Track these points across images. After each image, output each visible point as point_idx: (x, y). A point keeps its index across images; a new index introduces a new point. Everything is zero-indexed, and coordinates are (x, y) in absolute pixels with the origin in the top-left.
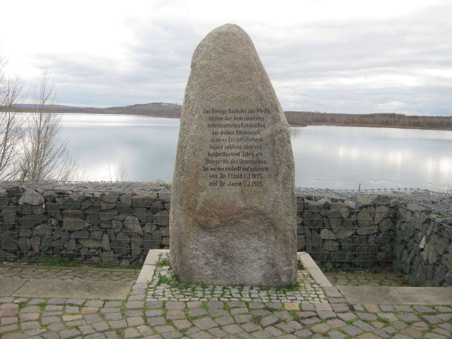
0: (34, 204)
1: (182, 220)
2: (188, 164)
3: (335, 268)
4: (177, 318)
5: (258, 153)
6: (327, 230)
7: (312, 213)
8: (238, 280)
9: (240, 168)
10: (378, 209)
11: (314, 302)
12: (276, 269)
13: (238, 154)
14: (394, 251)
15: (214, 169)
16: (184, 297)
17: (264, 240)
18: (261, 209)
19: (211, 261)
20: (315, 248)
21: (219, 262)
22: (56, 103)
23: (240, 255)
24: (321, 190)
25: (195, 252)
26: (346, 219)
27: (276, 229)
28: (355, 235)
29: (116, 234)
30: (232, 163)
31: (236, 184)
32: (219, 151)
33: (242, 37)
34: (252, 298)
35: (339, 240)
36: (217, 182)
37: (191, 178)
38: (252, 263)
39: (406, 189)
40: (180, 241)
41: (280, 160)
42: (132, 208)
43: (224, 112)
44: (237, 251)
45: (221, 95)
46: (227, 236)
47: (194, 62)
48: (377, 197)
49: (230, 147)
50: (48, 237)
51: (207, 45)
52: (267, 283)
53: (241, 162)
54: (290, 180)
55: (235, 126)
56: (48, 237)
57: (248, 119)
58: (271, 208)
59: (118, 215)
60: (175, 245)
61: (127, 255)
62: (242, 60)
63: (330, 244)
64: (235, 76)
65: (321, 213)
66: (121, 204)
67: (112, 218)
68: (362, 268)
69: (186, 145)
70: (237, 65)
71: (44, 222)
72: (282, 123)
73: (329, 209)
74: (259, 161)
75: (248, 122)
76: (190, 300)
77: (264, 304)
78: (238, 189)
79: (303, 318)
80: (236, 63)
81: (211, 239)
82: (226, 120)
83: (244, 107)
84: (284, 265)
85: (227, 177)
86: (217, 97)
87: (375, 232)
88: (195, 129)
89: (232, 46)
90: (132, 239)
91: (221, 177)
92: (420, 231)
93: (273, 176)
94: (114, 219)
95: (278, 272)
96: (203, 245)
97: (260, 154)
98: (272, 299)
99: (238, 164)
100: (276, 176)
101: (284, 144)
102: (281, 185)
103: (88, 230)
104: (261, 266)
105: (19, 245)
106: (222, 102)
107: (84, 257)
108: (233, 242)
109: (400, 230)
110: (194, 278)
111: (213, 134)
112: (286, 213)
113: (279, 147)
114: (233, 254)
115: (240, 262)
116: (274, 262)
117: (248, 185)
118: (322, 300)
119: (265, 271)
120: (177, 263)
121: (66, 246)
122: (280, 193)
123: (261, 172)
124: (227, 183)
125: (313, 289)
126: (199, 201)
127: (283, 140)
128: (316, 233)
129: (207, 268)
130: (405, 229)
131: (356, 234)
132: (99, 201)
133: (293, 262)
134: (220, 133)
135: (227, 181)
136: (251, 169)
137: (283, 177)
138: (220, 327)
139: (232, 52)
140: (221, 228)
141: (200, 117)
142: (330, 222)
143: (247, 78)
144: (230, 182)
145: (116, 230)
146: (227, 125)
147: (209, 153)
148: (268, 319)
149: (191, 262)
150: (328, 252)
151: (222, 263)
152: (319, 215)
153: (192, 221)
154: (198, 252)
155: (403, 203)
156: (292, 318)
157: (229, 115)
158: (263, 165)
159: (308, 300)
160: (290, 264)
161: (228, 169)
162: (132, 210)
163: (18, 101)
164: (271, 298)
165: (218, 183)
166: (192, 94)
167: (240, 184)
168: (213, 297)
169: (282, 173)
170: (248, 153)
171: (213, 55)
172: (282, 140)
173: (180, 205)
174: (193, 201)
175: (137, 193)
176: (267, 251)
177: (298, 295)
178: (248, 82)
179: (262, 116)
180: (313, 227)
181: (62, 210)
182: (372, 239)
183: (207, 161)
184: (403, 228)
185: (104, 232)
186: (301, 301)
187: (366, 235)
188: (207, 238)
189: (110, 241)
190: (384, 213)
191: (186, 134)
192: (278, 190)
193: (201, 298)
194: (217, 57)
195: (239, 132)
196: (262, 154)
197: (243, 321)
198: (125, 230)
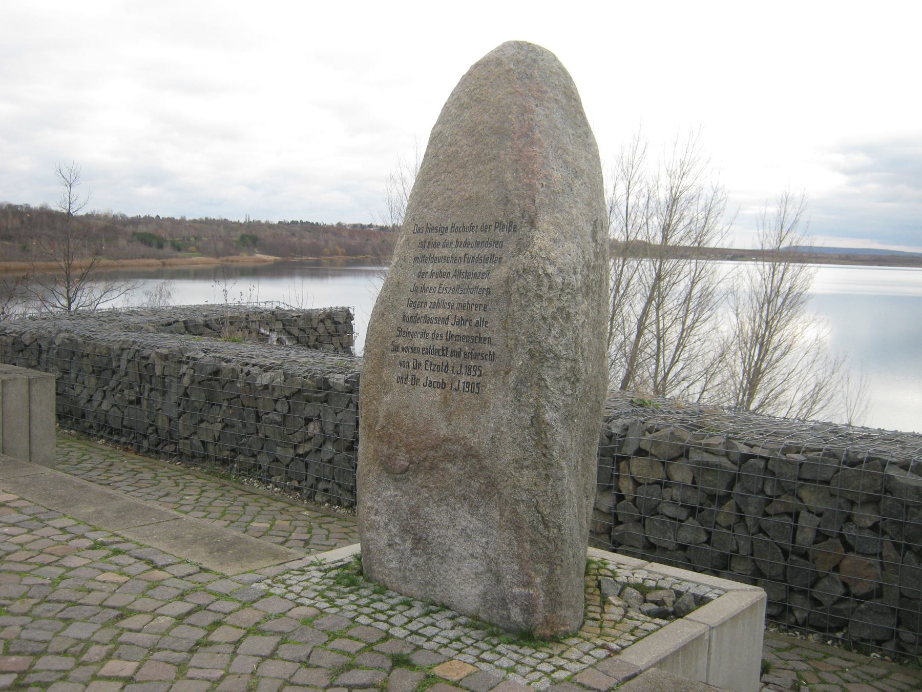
5: (479, 319)
8: (438, 595)
9: (447, 351)
13: (445, 320)
22: (805, 243)
25: (373, 517)
41: (516, 338)
43: (443, 230)
44: (433, 530)
46: (419, 494)
54: (532, 385)
57: (477, 244)
62: (492, 118)
74: (480, 338)
78: (437, 395)
81: (396, 496)
82: (443, 247)
84: (515, 581)
93: (502, 372)
99: (442, 342)
101: (527, 302)
108: (427, 509)
112: (517, 462)
113: (515, 309)
114: (427, 535)
115: (439, 556)
116: (498, 571)
122: (506, 413)
123: (482, 363)
124: (423, 380)
127: (527, 292)
129: (391, 554)
133: (538, 580)
134: (429, 275)
135: (425, 375)
137: (517, 378)
143: (491, 156)
147: (404, 316)
154: (378, 518)
158: (487, 348)
161: (426, 351)
163: (714, 242)
165: (410, 377)
167: (443, 385)
170: (462, 319)
176: (487, 543)
179: (500, 239)
195: (458, 274)
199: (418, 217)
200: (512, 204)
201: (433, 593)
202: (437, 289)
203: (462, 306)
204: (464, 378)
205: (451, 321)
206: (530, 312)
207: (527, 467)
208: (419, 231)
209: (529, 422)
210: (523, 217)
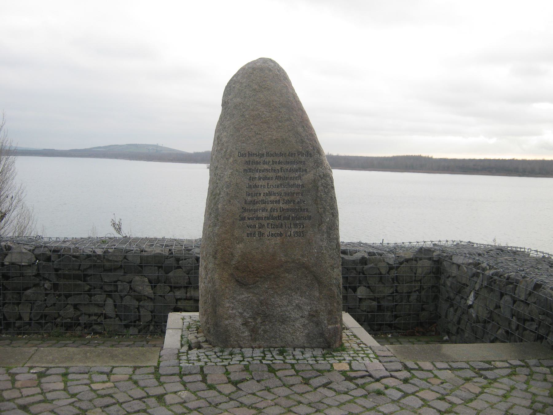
0: (23, 264)
1: (216, 276)
2: (223, 213)
3: (374, 331)
4: (219, 383)
6: (365, 287)
7: (348, 270)
10: (420, 263)
11: (364, 362)
12: (321, 327)
13: (278, 202)
14: (438, 310)
15: (252, 219)
16: (222, 360)
17: (307, 296)
18: (304, 262)
19: (249, 320)
20: (351, 308)
21: (258, 322)
23: (281, 313)
24: (354, 243)
25: (231, 312)
26: (385, 274)
27: (320, 283)
28: (396, 293)
29: (121, 297)
30: (272, 212)
31: (276, 235)
32: (257, 198)
33: (278, 73)
34: (298, 360)
35: (378, 298)
36: (255, 232)
37: (227, 228)
38: (294, 321)
39: (447, 241)
40: (214, 300)
42: (141, 267)
45: (258, 136)
46: (267, 293)
47: (226, 100)
48: (419, 250)
49: (270, 194)
50: (40, 303)
51: (241, 81)
52: (310, 343)
53: (281, 210)
55: (274, 171)
56: (40, 303)
57: (288, 163)
58: (314, 260)
59: (124, 275)
60: (208, 304)
61: (135, 322)
63: (367, 303)
64: (273, 116)
65: (357, 269)
66: (128, 263)
67: (117, 279)
68: (403, 330)
69: (220, 192)
70: (274, 103)
71: (35, 285)
72: (325, 167)
73: (366, 264)
74: (301, 209)
75: (288, 167)
76: (229, 364)
77: (311, 365)
78: (278, 240)
79: (355, 378)
80: (273, 101)
81: (249, 297)
82: (264, 164)
83: (283, 150)
85: (266, 227)
86: (254, 139)
87: (416, 289)
88: (230, 175)
89: (268, 82)
90: (141, 303)
91: (260, 227)
92: (467, 286)
94: (119, 280)
95: (322, 331)
96: (240, 303)
97: (302, 201)
98: (318, 361)
100: (319, 225)
102: (325, 235)
103: (88, 294)
104: (304, 325)
105: (5, 313)
106: (259, 145)
107: (83, 326)
108: (273, 299)
109: (444, 286)
110: (230, 341)
111: (249, 180)
112: (331, 266)
113: (322, 194)
114: (274, 313)
116: (319, 320)
117: (290, 235)
118: (372, 359)
119: (309, 330)
120: (211, 325)
121: (61, 313)
124: (267, 233)
125: (360, 349)
126: (235, 254)
127: (327, 186)
128: (352, 292)
130: (451, 284)
131: (397, 292)
132: (102, 259)
134: (258, 178)
135: (267, 231)
136: (292, 218)
137: (327, 226)
138: (268, 390)
139: (269, 90)
140: (260, 284)
141: (235, 161)
142: (368, 279)
144: (270, 232)
145: (122, 293)
146: (265, 169)
147: (246, 201)
148: (318, 380)
149: (227, 322)
150: (365, 313)
151: (261, 323)
152: (354, 271)
153: (227, 276)
154: (234, 311)
155: (447, 256)
156: (343, 378)
157: (268, 159)
158: (306, 214)
159: (357, 361)
160: (335, 322)
161: (268, 218)
162: (141, 269)
164: (318, 359)
165: (257, 233)
166: (225, 135)
167: (281, 235)
168: (254, 360)
169: (326, 222)
171: (247, 93)
172: (326, 186)
173: (213, 260)
174: (229, 254)
175: (146, 249)
176: (311, 308)
177: (346, 355)
178: (287, 123)
180: (348, 285)
181: (56, 270)
182: (414, 296)
183: (244, 209)
184: (449, 284)
185: (107, 296)
186: (350, 361)
187: (407, 293)
188: (245, 295)
189: (115, 306)
190: (427, 268)
191: (220, 180)
192: (322, 241)
193: (241, 361)
194: (252, 94)
195: (277, 178)
196: (304, 201)
197: (291, 383)
198: (133, 293)
199: (240, 148)
200: (306, 143)
201: (274, 342)
202: (266, 186)
203: (287, 194)
204: (293, 230)
205: (281, 202)
206: (330, 195)
207: (336, 268)
208: (242, 155)
209: (335, 246)
210: (314, 149)
